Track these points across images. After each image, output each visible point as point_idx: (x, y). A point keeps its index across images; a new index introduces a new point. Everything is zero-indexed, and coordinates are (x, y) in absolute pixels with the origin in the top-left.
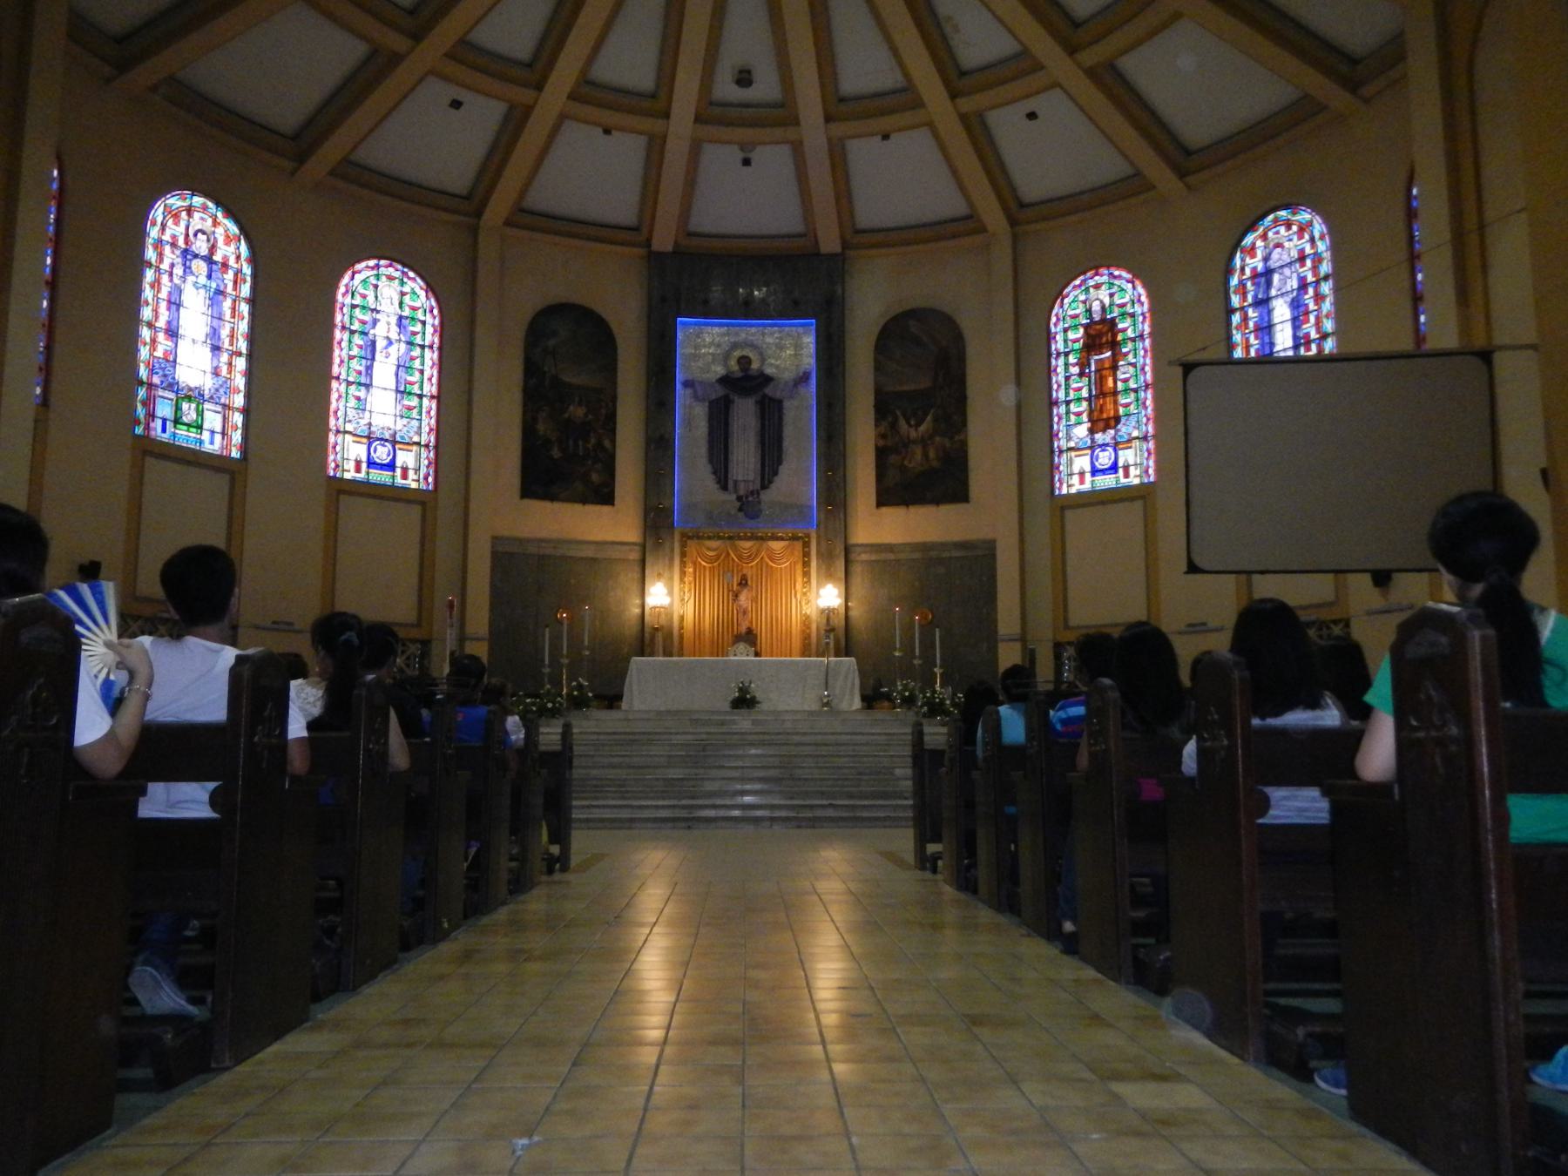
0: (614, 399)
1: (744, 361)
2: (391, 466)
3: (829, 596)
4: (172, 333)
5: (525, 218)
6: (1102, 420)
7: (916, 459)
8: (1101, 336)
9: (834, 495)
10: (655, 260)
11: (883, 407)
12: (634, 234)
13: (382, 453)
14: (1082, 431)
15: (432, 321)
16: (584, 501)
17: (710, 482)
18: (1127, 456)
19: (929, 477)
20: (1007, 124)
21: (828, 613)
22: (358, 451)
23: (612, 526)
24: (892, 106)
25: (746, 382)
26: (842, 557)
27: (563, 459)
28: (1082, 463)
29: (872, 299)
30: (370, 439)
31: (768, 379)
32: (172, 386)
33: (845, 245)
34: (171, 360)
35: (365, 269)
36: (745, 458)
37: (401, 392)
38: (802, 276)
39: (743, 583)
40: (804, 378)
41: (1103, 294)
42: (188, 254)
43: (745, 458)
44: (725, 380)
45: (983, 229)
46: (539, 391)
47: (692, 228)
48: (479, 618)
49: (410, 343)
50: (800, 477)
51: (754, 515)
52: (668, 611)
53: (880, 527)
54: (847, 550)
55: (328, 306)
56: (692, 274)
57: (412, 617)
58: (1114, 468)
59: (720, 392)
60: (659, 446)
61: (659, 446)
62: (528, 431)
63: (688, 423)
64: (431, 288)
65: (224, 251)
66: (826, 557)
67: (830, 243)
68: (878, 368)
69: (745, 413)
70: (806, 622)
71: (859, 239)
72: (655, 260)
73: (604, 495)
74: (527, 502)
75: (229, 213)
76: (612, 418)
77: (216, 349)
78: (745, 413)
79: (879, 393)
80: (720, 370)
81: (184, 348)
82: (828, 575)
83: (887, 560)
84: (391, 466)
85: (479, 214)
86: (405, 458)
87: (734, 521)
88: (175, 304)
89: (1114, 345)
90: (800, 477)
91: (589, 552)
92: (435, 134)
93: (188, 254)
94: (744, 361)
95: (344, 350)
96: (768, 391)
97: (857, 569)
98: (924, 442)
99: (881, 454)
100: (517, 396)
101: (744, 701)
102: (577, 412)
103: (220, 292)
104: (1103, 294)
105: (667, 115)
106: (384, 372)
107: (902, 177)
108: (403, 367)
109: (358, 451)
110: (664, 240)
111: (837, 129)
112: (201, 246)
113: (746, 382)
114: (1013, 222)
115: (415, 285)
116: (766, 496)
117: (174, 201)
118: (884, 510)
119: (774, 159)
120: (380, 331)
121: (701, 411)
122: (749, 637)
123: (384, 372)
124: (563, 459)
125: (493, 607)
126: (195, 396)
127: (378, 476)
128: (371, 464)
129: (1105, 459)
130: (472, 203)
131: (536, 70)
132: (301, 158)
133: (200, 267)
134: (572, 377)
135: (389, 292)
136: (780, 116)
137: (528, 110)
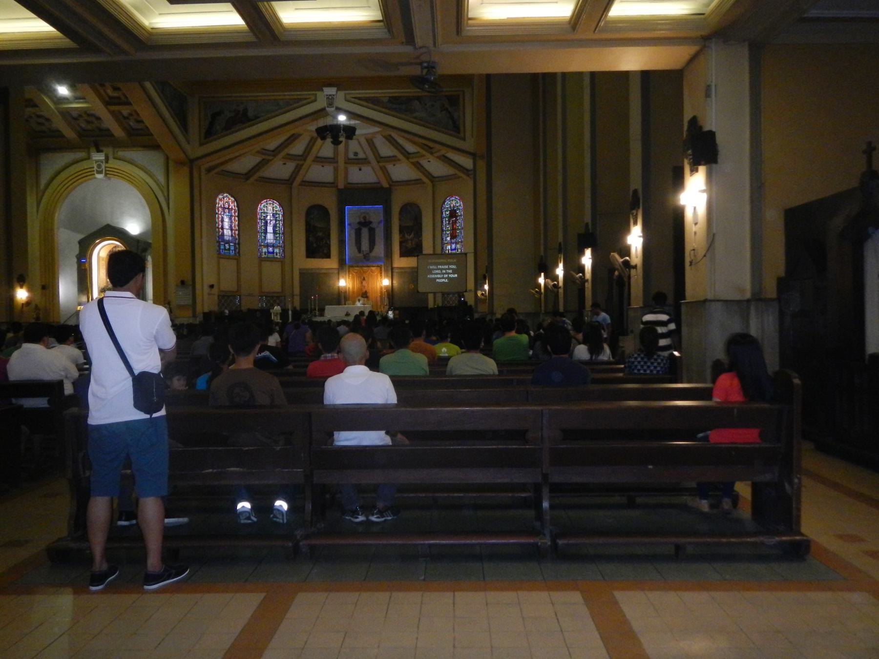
0: (329, 230)
1: (365, 218)
2: (273, 253)
3: (386, 282)
4: (222, 228)
5: (305, 183)
6: (453, 236)
7: (409, 245)
8: (453, 213)
9: (389, 255)
10: (340, 192)
11: (402, 230)
12: (333, 184)
13: (271, 249)
14: (449, 239)
15: (281, 213)
16: (322, 257)
17: (356, 251)
18: (458, 246)
19: (412, 249)
20: (424, 162)
21: (386, 287)
22: (265, 250)
23: (331, 264)
24: (392, 159)
25: (365, 223)
26: (391, 271)
27: (317, 247)
28: (449, 247)
29: (398, 200)
30: (267, 246)
31: (370, 223)
32: (224, 240)
33: (390, 185)
34: (223, 234)
35: (264, 203)
36: (365, 246)
37: (275, 232)
38: (378, 194)
39: (364, 279)
40: (381, 222)
41: (454, 202)
42: (224, 208)
43: (365, 246)
44: (360, 223)
45: (424, 183)
46: (310, 229)
47: (349, 181)
48: (297, 290)
49: (276, 220)
50: (379, 249)
51: (368, 260)
52: (345, 287)
53: (400, 262)
54: (392, 269)
55: (256, 214)
56: (350, 194)
57: (280, 290)
58: (455, 249)
59: (357, 226)
60: (342, 242)
61: (342, 242)
62: (307, 241)
63: (350, 235)
64: (280, 205)
65: (232, 205)
66: (386, 271)
67: (385, 185)
68: (400, 220)
69: (365, 232)
70: (381, 288)
71: (393, 184)
72: (340, 191)
73: (328, 256)
74: (309, 260)
75: (232, 196)
76: (329, 235)
77: (232, 230)
78: (365, 232)
79: (400, 226)
80: (358, 220)
81: (225, 231)
82: (387, 276)
83: (403, 271)
84: (273, 253)
85: (292, 184)
86: (277, 250)
87: (362, 262)
88: (222, 221)
89: (456, 217)
90: (379, 249)
91: (323, 271)
92: (280, 169)
93: (224, 208)
94: (365, 218)
95: (261, 224)
96: (371, 226)
97: (395, 274)
98: (411, 240)
99: (401, 243)
100: (304, 231)
101: (347, 315)
102: (320, 234)
103: (232, 216)
104: (454, 202)
105: (337, 162)
106: (270, 229)
107: (402, 171)
108: (275, 226)
109: (265, 250)
110: (341, 186)
111: (381, 164)
112: (227, 206)
113: (365, 223)
114: (432, 182)
115: (276, 204)
116: (373, 254)
117: (221, 197)
118: (402, 259)
119: (366, 169)
120: (268, 218)
121: (353, 232)
122: (365, 295)
123: (270, 229)
124: (317, 247)
125: (301, 287)
126: (228, 242)
127: (270, 256)
128: (269, 252)
129: (453, 246)
130: (289, 182)
131: (304, 157)
132: (247, 179)
133: (227, 211)
134: (320, 225)
135: (270, 208)
136: (365, 161)
137: (302, 165)
